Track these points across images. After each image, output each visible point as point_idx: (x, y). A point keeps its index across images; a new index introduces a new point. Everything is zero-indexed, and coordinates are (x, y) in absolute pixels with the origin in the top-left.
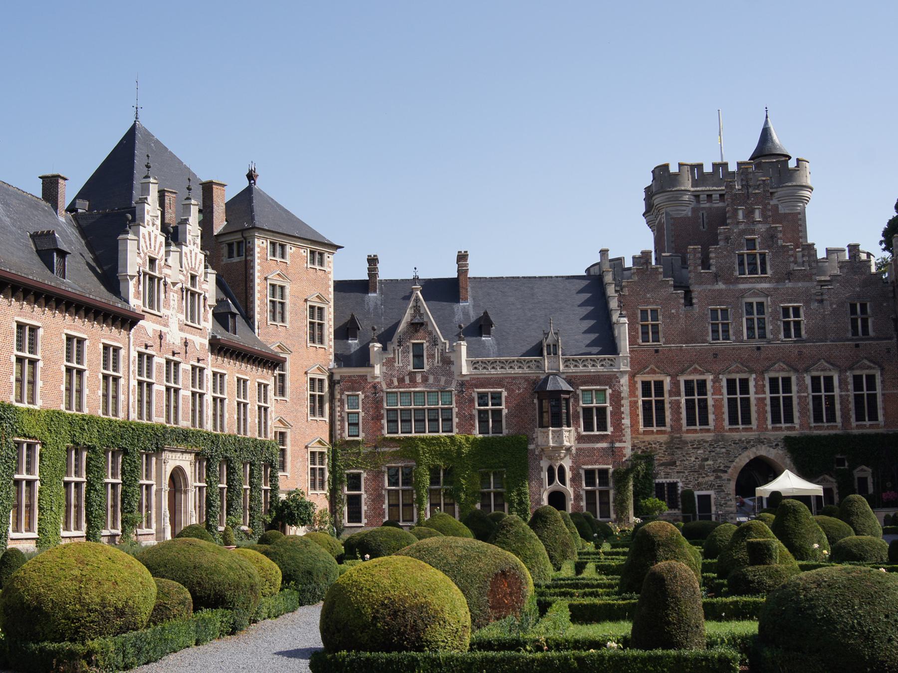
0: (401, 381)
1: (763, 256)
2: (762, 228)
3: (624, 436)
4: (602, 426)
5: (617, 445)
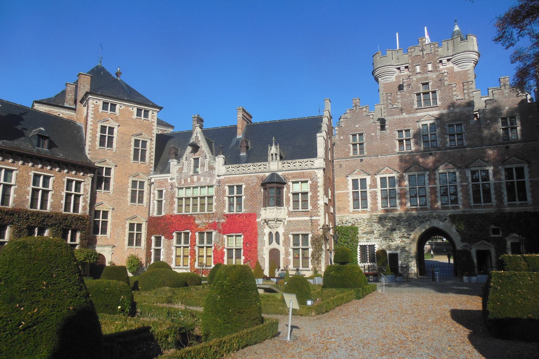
0: (186, 180)
1: (434, 92)
2: (434, 75)
3: (319, 212)
4: (305, 206)
5: (314, 218)
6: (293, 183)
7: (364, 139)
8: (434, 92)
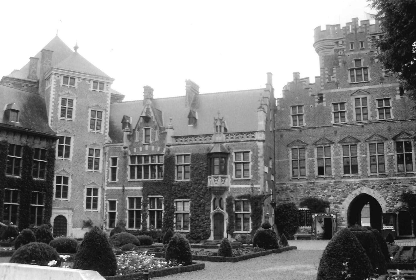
6: (236, 153)
7: (303, 111)
8: (366, 68)
